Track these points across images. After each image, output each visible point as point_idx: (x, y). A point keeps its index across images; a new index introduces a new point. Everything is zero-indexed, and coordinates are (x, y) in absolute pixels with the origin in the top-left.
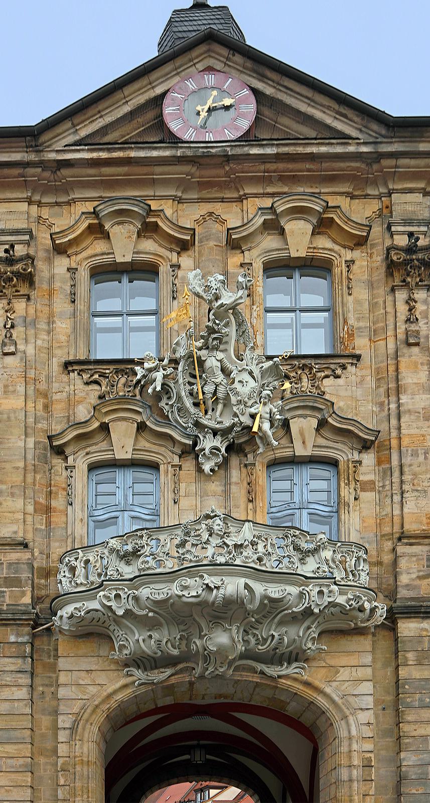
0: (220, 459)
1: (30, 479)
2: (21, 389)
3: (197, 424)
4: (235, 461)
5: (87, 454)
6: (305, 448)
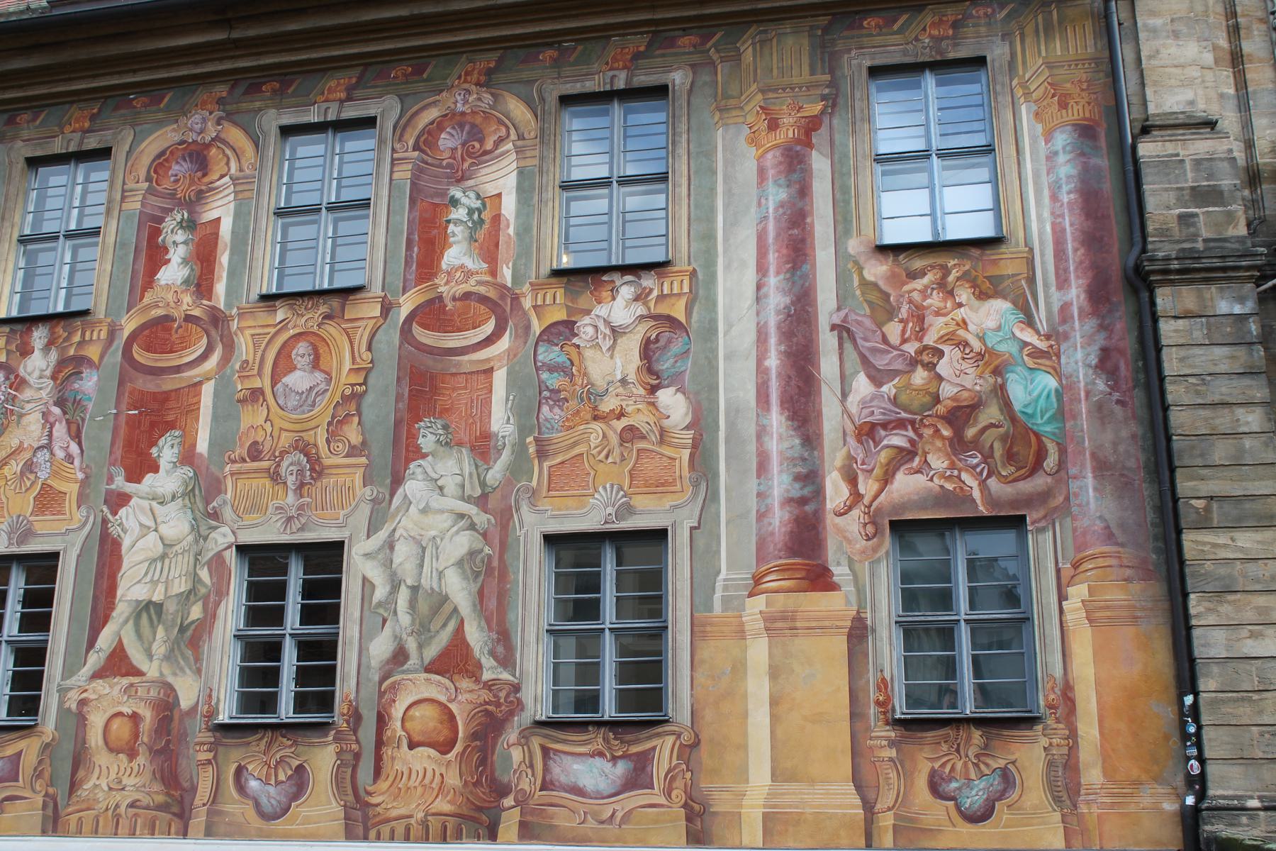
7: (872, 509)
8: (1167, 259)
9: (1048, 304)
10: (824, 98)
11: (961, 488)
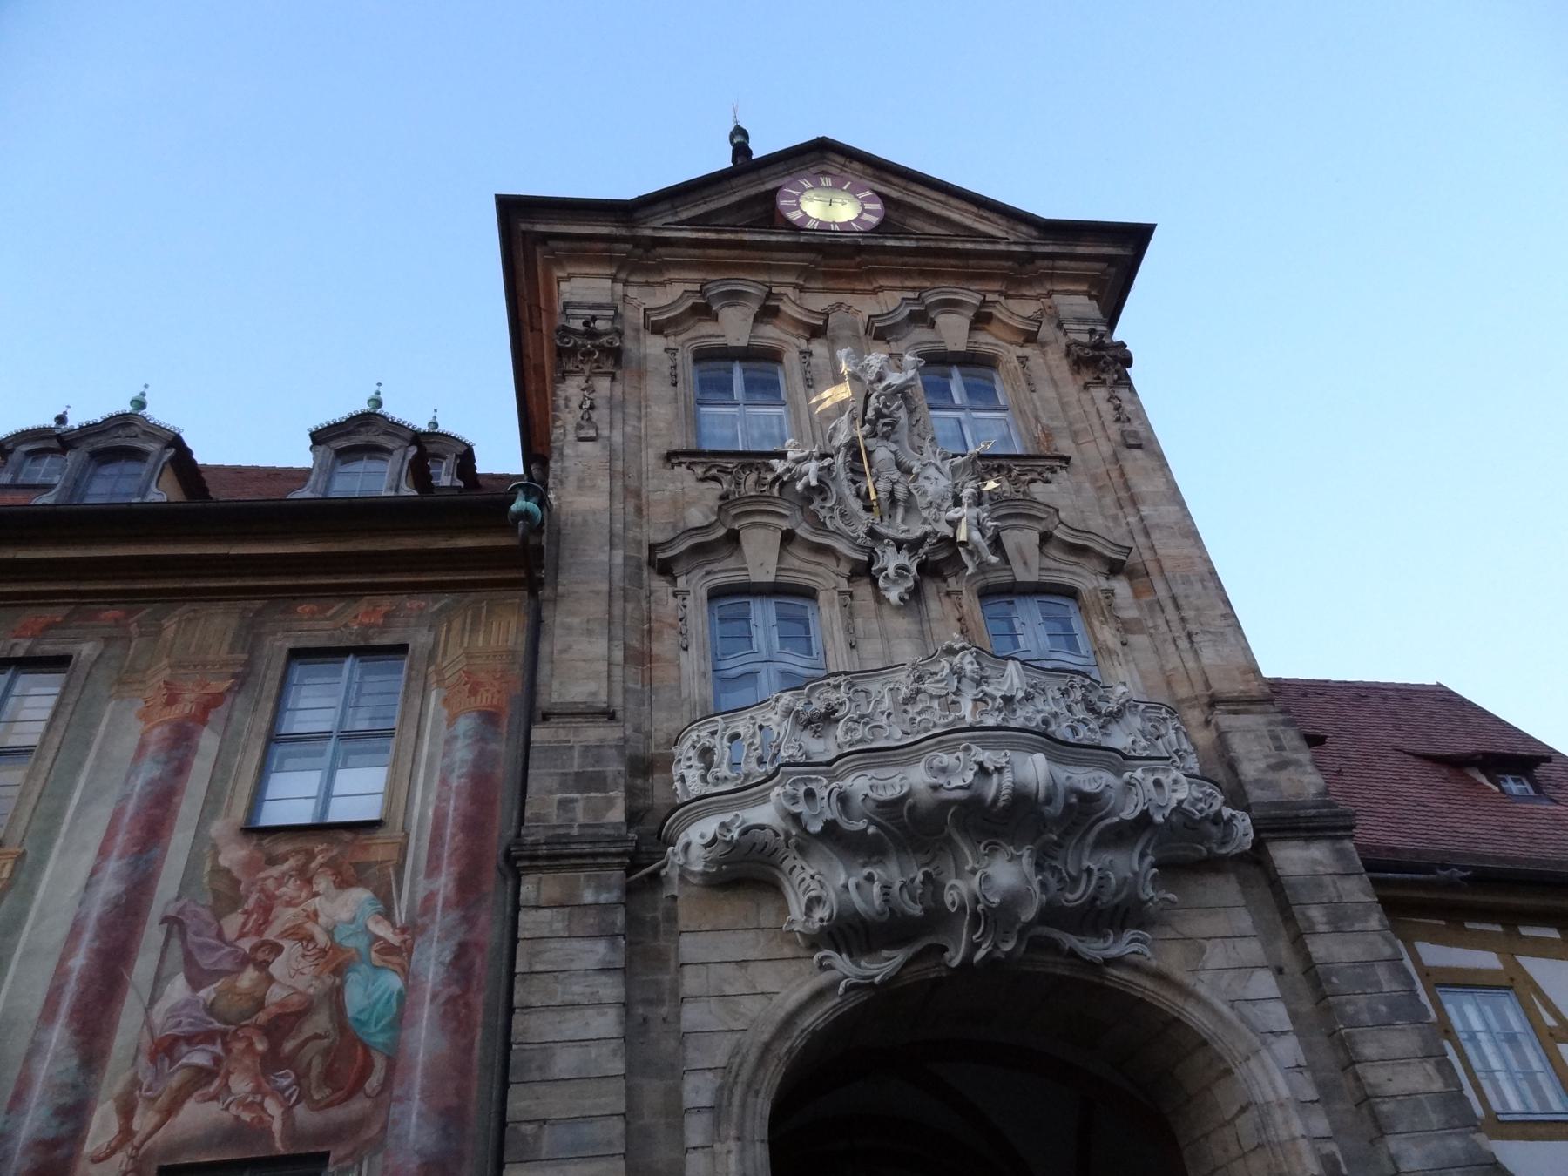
0: (911, 583)
1: (617, 611)
2: (603, 483)
3: (872, 533)
4: (930, 588)
5: (708, 573)
6: (1029, 571)
7: (141, 1152)
8: (536, 844)
9: (412, 893)
10: (234, 676)
11: (261, 1119)
